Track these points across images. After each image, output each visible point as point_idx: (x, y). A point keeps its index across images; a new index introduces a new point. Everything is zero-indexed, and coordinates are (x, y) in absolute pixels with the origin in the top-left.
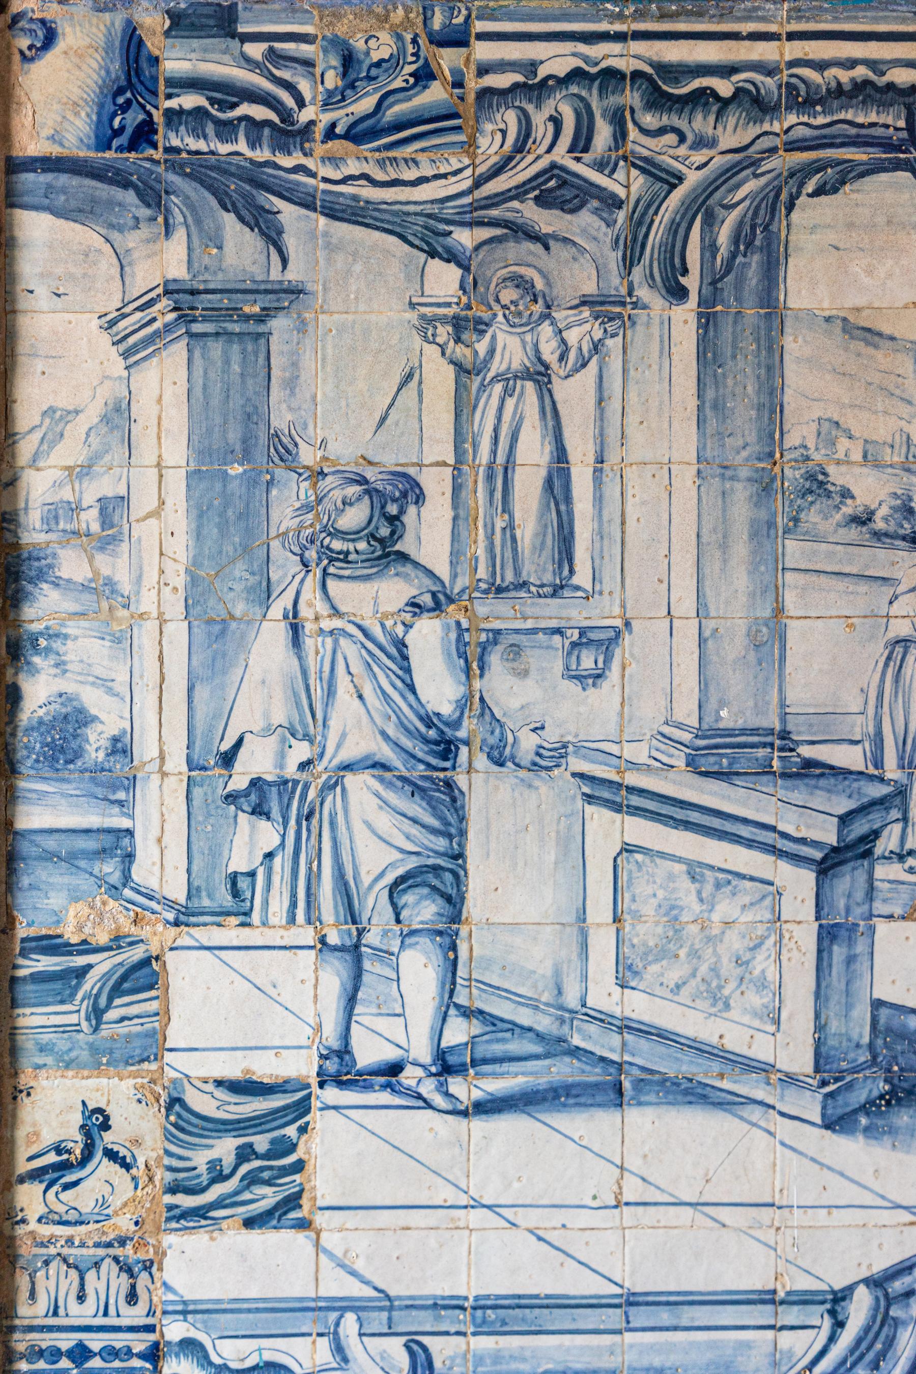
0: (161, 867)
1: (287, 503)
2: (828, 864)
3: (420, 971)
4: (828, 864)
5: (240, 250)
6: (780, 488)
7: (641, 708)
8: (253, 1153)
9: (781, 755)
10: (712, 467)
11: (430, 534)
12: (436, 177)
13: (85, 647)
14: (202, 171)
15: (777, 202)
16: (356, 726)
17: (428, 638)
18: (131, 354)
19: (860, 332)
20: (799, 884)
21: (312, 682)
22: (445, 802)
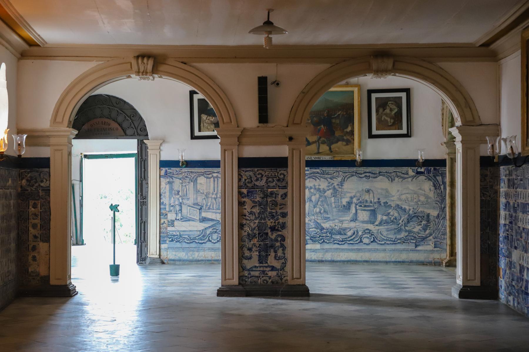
0: (167, 209)
1: (173, 192)
2: (200, 209)
3: (180, 215)
4: (200, 209)
5: (171, 180)
6: (197, 191)
7: (190, 202)
8: (172, 223)
9: (197, 204)
10: (194, 190)
11: (180, 193)
12: (181, 176)
13: (164, 199)
14: (169, 176)
15: (197, 177)
16: (177, 203)
17: (180, 198)
18: (166, 185)
19: (201, 184)
20: (198, 210)
21: (175, 200)
22: (181, 206)
